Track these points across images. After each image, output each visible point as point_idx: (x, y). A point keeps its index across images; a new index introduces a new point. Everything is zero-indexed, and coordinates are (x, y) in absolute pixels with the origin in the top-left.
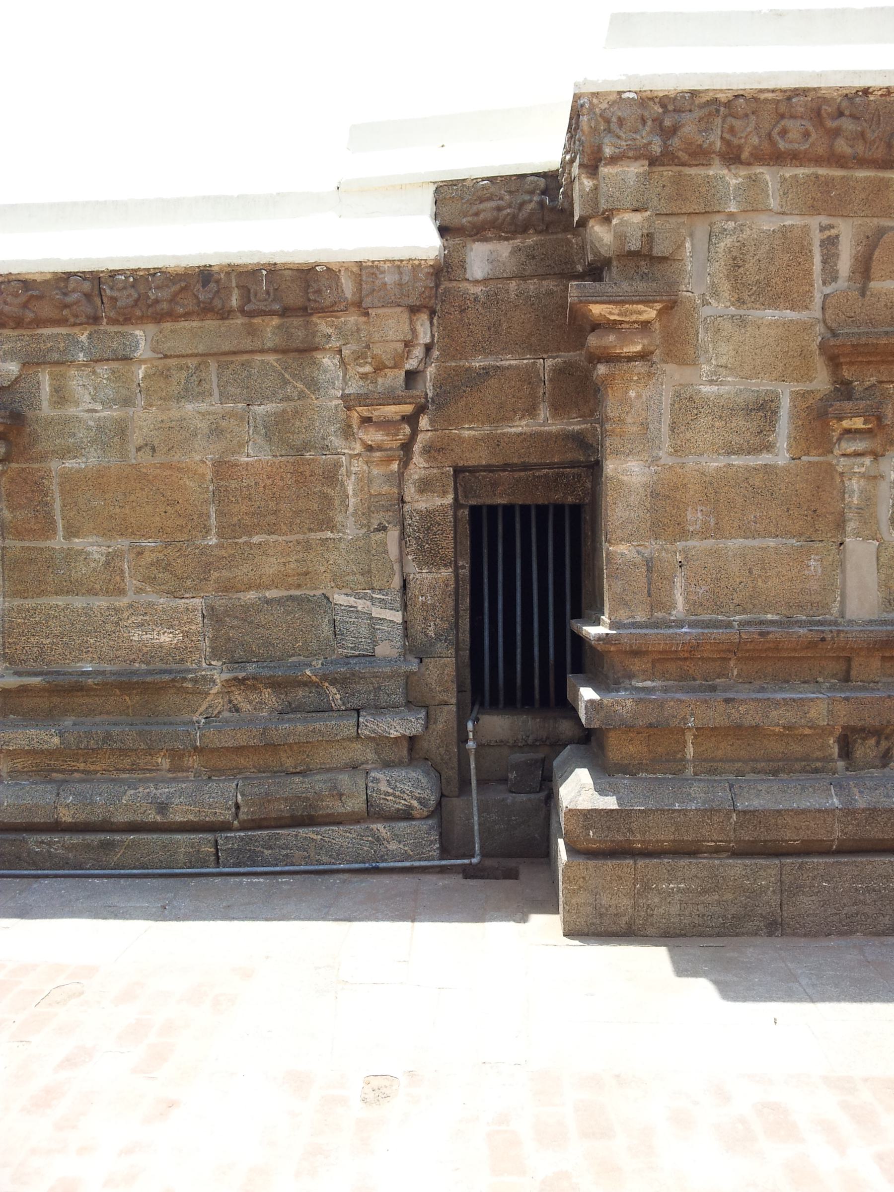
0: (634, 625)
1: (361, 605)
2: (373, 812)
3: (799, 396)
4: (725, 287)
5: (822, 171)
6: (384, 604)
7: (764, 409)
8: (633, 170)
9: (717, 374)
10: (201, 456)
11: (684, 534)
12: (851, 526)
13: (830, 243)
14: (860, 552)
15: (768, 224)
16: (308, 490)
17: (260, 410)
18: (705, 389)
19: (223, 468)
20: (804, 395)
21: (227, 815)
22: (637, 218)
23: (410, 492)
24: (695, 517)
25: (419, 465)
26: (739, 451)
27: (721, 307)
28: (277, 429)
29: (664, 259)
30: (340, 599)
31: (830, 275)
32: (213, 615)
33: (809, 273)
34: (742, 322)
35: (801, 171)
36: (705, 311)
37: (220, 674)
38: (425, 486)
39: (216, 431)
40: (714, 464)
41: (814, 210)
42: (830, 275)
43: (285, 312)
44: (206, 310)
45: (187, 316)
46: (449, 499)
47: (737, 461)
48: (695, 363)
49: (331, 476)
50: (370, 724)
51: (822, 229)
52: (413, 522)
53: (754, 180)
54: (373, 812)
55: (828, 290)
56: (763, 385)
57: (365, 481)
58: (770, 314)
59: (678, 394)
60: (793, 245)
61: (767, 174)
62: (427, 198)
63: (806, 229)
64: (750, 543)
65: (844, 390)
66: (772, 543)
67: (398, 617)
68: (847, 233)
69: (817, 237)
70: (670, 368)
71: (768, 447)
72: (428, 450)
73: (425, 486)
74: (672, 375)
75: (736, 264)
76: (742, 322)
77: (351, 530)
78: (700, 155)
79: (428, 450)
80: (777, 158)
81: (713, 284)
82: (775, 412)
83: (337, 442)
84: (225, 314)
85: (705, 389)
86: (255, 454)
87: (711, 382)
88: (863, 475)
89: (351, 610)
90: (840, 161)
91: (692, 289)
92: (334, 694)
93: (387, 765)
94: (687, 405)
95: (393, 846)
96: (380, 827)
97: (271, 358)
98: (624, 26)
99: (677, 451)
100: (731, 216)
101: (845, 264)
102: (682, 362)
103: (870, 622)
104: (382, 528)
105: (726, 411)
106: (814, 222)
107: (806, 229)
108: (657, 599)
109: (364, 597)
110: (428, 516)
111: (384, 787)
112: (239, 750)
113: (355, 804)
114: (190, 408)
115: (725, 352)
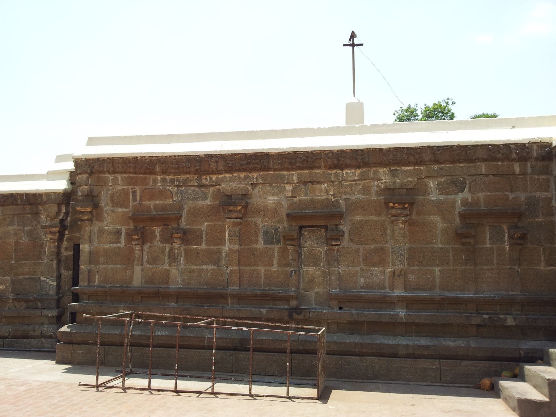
0: (84, 286)
1: (47, 280)
2: (42, 336)
3: (126, 229)
4: (110, 203)
5: (131, 175)
6: (52, 280)
7: (119, 232)
8: (85, 176)
9: (108, 225)
10: (12, 240)
11: (99, 264)
12: (136, 262)
13: (134, 192)
14: (137, 269)
15: (120, 188)
16: (36, 249)
17: (26, 228)
18: (106, 228)
19: (17, 243)
20: (128, 229)
21: (6, 334)
22: (86, 187)
23: (63, 250)
24: (102, 259)
25: (65, 244)
26: (113, 243)
27: (109, 208)
28: (30, 234)
29: (96, 196)
30: (43, 278)
31: (135, 200)
32: (12, 282)
33: (129, 199)
34: (113, 211)
35: (126, 175)
36: (105, 209)
37: (11, 296)
38: (66, 249)
39: (16, 234)
40: (107, 246)
41: (130, 184)
42: (135, 200)
43: (30, 204)
44: (12, 204)
45: (8, 205)
46: (72, 253)
47: (112, 246)
48: (102, 221)
49: (42, 246)
50: (45, 312)
51: (132, 189)
52: (63, 259)
53: (116, 177)
54: (42, 336)
55: (134, 204)
56: (119, 227)
57: (50, 247)
58: (120, 210)
59: (99, 229)
60: (125, 193)
61: (119, 176)
62: (67, 176)
63: (128, 189)
64: (114, 266)
65: (136, 229)
66: (119, 266)
67: (55, 284)
68: (138, 189)
69: (131, 191)
70: (97, 222)
71: (119, 242)
72: (68, 240)
73: (66, 249)
74: (97, 225)
75: (112, 197)
76: (113, 211)
77: (45, 261)
78: (102, 172)
79: (68, 240)
80: (121, 173)
81: (107, 202)
82: (121, 234)
83: (43, 237)
84: (17, 205)
85: (106, 228)
86: (24, 240)
87: (107, 226)
88: (138, 250)
89: (45, 282)
90: (135, 173)
91: (102, 204)
92: (39, 304)
93: (51, 324)
94: (101, 231)
95: (46, 345)
96: (43, 340)
97: (29, 215)
98: (92, 141)
99: (99, 243)
100: (111, 186)
101: (138, 197)
102: (100, 221)
103: (139, 287)
104: (52, 260)
105: (110, 233)
106: (130, 187)
107: (128, 189)
108: (90, 280)
109: (48, 278)
110: (67, 257)
111: (45, 329)
112: (14, 317)
113: (38, 333)
114: (10, 228)
115: (109, 219)
